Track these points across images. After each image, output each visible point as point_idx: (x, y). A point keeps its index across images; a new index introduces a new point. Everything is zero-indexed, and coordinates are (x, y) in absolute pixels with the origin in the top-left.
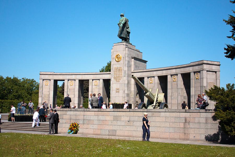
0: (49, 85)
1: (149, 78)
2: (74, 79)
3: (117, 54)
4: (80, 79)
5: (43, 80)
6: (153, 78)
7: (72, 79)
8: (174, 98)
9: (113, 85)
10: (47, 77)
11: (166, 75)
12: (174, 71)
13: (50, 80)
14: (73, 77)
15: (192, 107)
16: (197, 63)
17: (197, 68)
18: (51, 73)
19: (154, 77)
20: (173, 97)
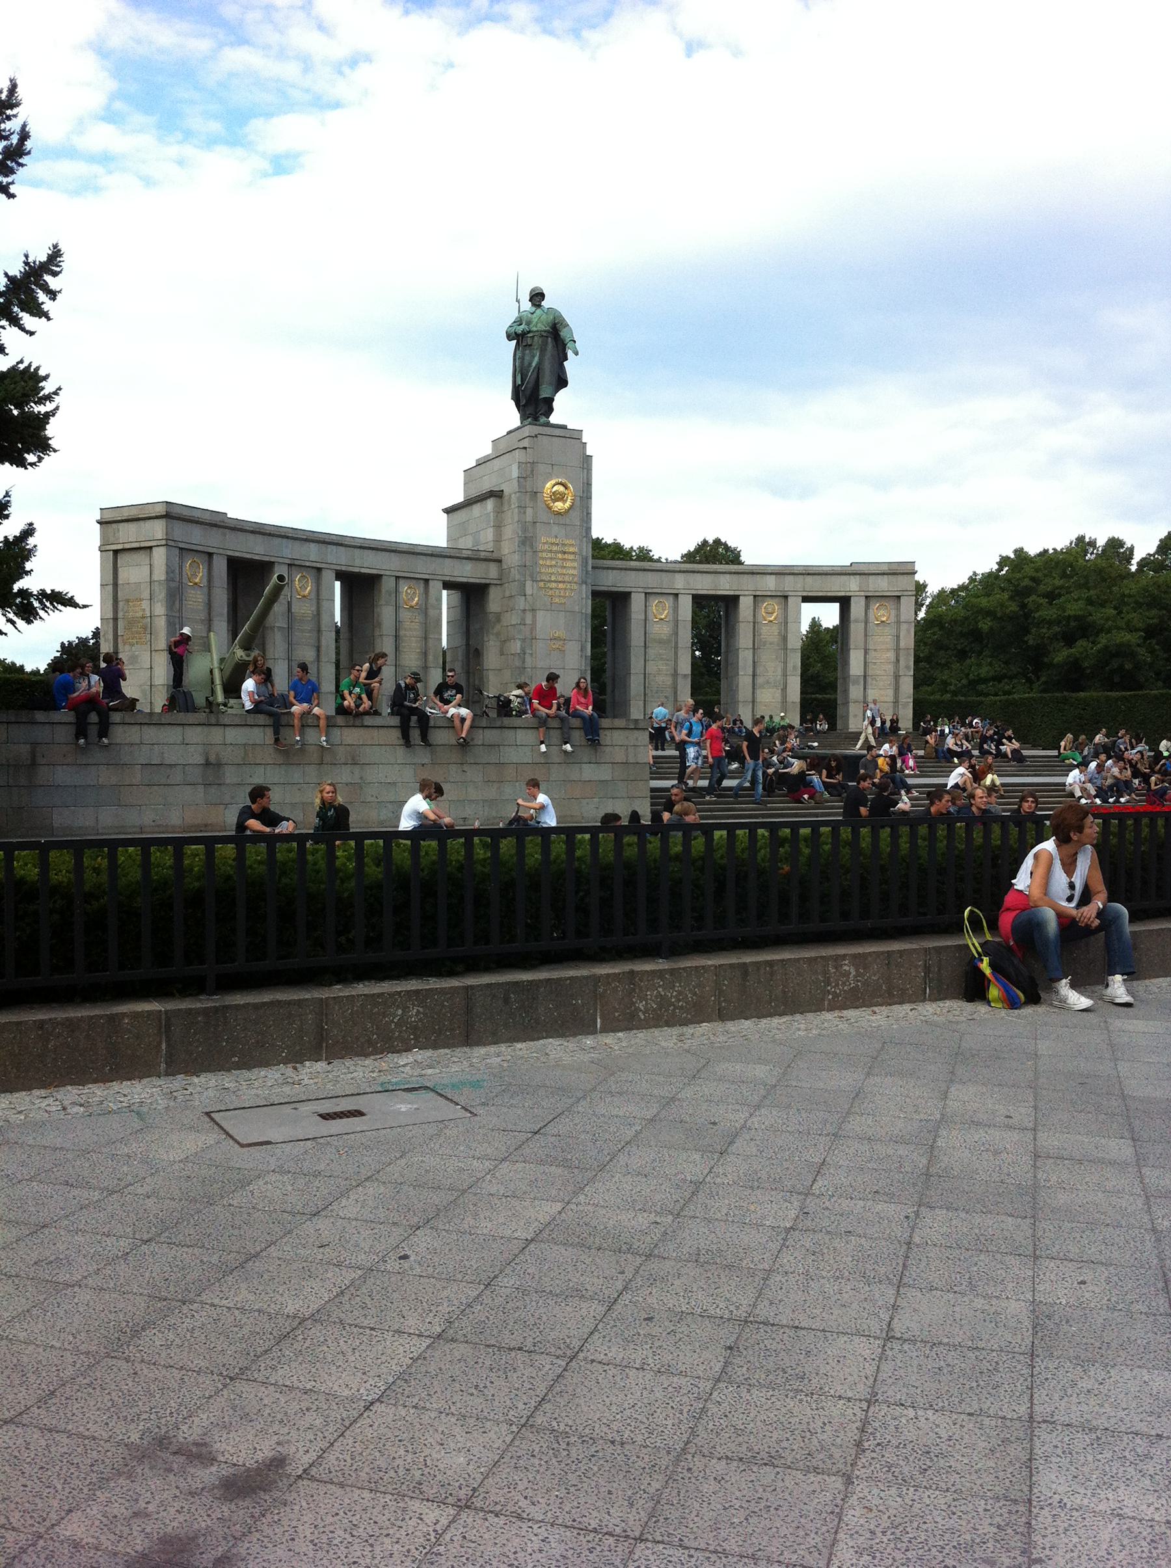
0: (205, 583)
1: (651, 598)
2: (318, 565)
3: (553, 482)
4: (344, 568)
5: (181, 549)
6: (668, 602)
7: (308, 564)
8: (768, 682)
9: (534, 617)
10: (196, 537)
11: (732, 593)
12: (770, 583)
13: (210, 555)
14: (312, 554)
15: (855, 716)
16: (885, 568)
17: (882, 585)
18: (216, 519)
19: (676, 595)
20: (760, 680)
